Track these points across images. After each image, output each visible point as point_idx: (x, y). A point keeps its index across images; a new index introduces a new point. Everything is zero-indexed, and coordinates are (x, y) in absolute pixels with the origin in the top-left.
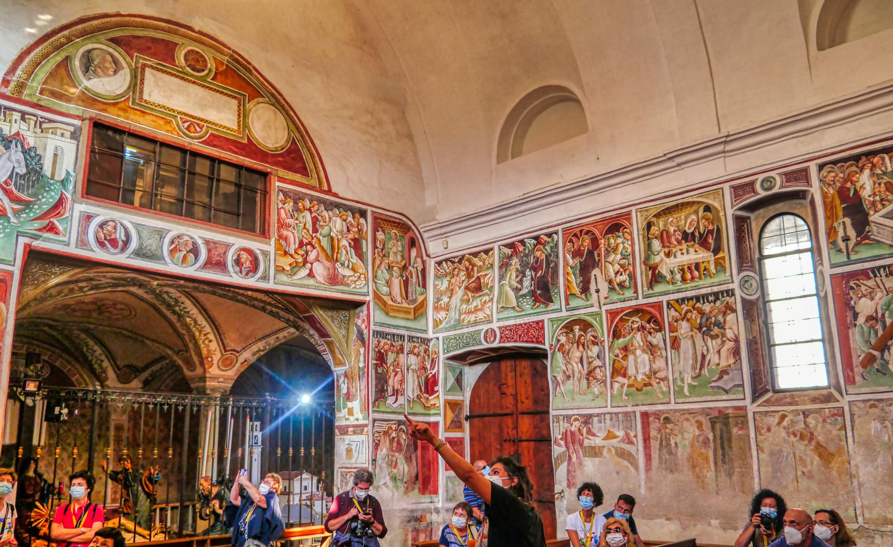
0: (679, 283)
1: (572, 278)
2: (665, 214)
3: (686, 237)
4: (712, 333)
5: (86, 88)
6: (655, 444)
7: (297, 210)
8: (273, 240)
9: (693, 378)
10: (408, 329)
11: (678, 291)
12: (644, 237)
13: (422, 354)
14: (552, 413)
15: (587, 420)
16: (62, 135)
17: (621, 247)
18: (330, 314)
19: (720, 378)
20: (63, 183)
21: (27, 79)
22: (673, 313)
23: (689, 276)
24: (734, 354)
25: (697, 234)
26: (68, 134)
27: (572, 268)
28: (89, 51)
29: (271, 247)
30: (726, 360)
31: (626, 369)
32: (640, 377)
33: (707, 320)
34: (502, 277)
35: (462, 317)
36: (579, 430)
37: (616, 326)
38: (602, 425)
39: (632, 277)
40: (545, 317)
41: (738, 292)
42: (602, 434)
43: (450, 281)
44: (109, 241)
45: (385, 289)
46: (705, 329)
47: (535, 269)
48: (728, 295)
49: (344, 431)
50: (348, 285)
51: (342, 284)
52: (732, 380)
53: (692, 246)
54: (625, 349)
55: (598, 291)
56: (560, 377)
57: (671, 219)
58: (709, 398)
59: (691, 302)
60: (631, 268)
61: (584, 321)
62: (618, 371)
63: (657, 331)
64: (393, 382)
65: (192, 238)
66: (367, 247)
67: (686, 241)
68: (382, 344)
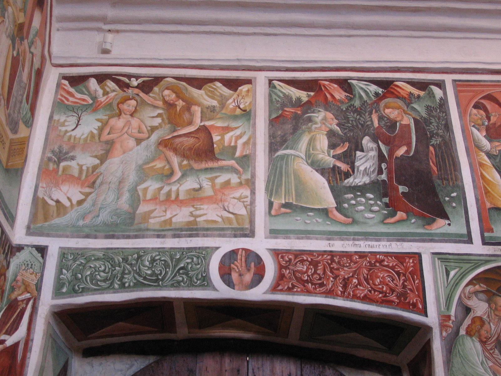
27: (489, 155)
35: (143, 208)
40: (426, 249)
43: (105, 124)
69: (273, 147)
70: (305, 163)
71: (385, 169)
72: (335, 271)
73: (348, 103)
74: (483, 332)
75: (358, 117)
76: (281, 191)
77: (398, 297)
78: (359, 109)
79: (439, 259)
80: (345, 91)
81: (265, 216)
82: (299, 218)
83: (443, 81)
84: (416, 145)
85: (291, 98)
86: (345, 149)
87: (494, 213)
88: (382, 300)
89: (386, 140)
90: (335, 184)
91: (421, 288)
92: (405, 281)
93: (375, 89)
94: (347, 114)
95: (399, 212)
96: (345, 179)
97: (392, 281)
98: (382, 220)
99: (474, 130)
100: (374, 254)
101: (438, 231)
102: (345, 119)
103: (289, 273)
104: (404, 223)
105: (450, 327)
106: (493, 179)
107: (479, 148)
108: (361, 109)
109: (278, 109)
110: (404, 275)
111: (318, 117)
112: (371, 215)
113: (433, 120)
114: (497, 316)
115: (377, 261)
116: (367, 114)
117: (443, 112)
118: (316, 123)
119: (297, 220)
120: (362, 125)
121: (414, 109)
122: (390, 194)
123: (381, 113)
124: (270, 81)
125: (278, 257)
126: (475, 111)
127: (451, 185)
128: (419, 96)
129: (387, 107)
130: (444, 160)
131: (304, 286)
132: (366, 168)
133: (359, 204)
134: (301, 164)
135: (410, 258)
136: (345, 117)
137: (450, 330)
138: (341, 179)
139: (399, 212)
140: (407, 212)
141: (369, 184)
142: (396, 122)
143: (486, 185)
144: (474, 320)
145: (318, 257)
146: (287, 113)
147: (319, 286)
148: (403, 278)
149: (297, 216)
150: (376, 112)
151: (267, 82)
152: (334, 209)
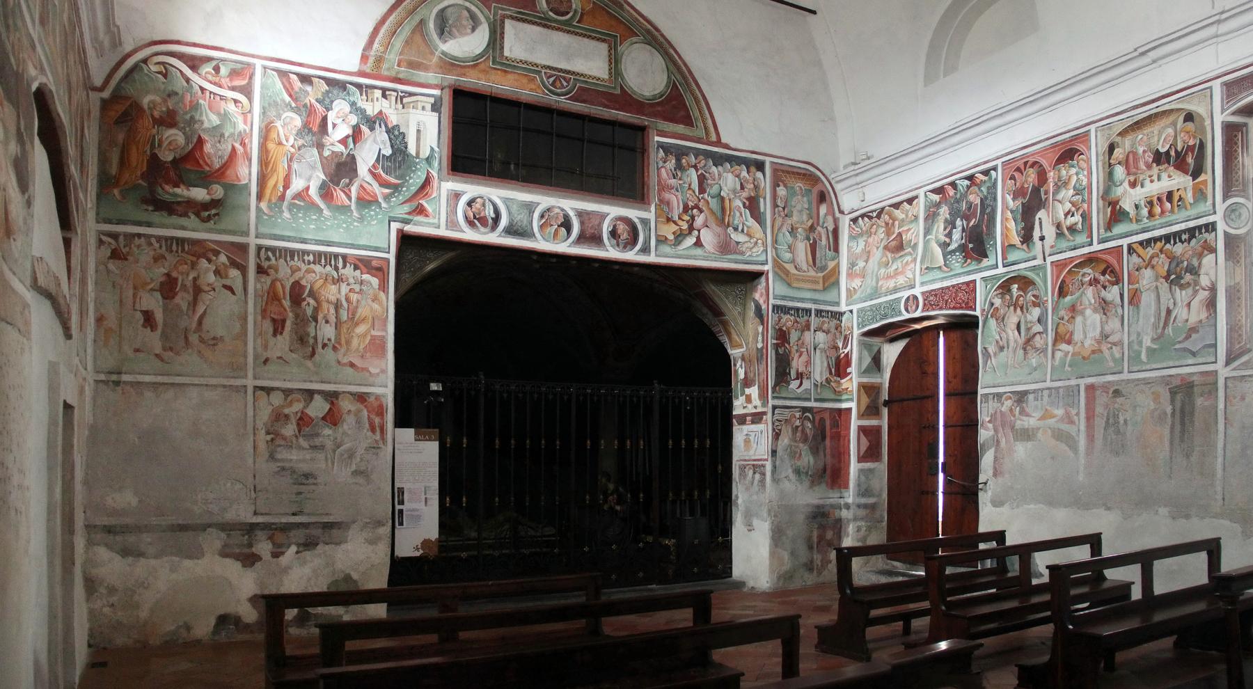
0: (1145, 220)
2: (1133, 130)
3: (1159, 158)
5: (443, 53)
6: (1099, 423)
7: (679, 167)
8: (653, 208)
9: (1153, 340)
10: (815, 301)
11: (1144, 231)
13: (833, 330)
14: (981, 391)
15: (1021, 397)
16: (423, 108)
17: (1074, 178)
18: (723, 288)
19: (1188, 337)
20: (429, 160)
21: (384, 52)
22: (1135, 258)
23: (1157, 210)
24: (1207, 306)
25: (1173, 153)
26: (429, 107)
27: (1012, 212)
28: (443, 10)
29: (651, 215)
30: (1197, 314)
31: (1072, 333)
32: (1088, 343)
33: (1177, 265)
34: (927, 231)
36: (1011, 410)
37: (1063, 282)
38: (1039, 403)
39: (1086, 217)
40: (977, 277)
41: (1221, 227)
42: (1037, 415)
44: (479, 220)
45: (788, 256)
47: (967, 218)
48: (1207, 231)
49: (742, 420)
50: (743, 253)
51: (735, 253)
54: (1073, 308)
55: (1042, 238)
56: (991, 349)
58: (1171, 364)
59: (1159, 245)
60: (1085, 206)
61: (1025, 277)
62: (1062, 337)
63: (1113, 284)
64: (797, 364)
65: (563, 210)
66: (766, 206)
68: (783, 321)
69: (925, 235)
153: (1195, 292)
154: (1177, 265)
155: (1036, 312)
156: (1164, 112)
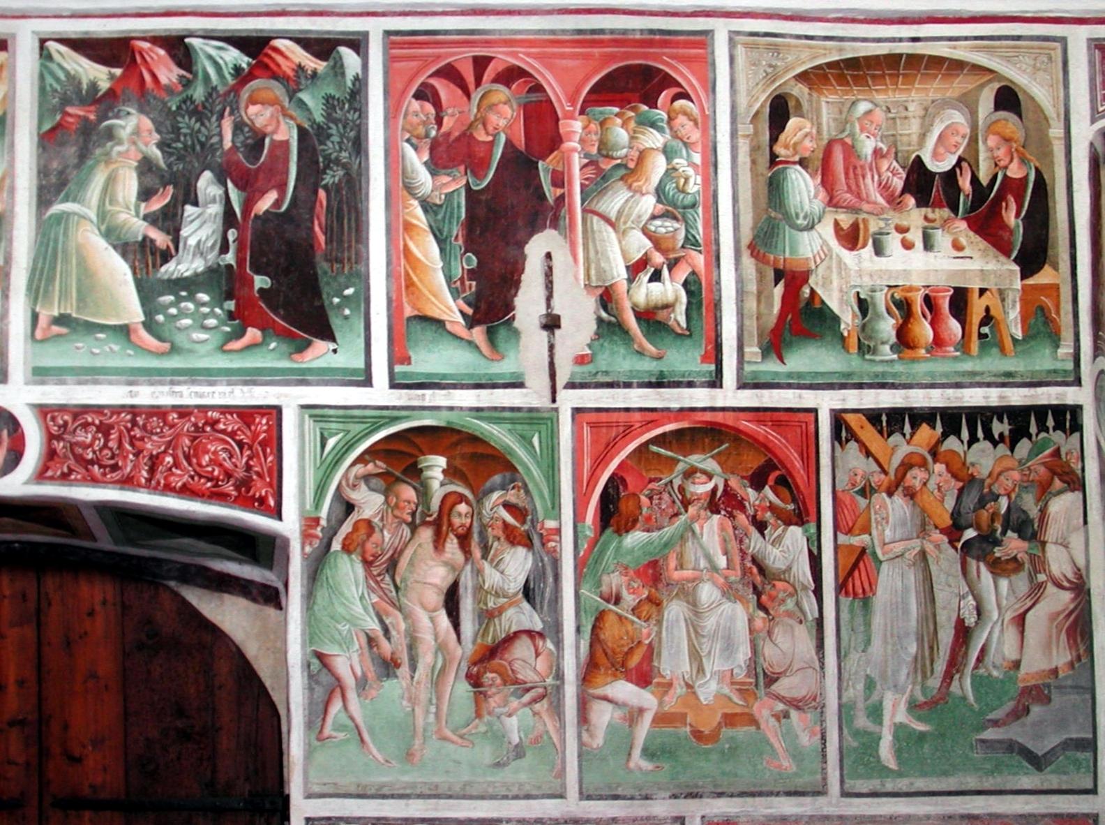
0: (886, 352)
1: (428, 250)
2: (842, 80)
3: (921, 184)
4: (998, 552)
9: (913, 707)
12: (755, 149)
17: (658, 166)
23: (924, 330)
24: (1071, 633)
25: (965, 183)
27: (427, 206)
30: (1041, 653)
31: (651, 653)
32: (708, 690)
33: (982, 503)
34: (52, 187)
39: (700, 295)
46: (970, 534)
48: (1059, 426)
52: (1062, 723)
53: (945, 223)
55: (552, 324)
56: (348, 663)
57: (863, 107)
58: (972, 782)
59: (924, 429)
60: (699, 260)
61: (474, 439)
67: (922, 202)
70: (97, 232)
71: (234, 241)
72: (138, 443)
73: (181, 93)
74: (370, 546)
75: (198, 125)
76: (54, 290)
77: (237, 488)
78: (200, 108)
79: (311, 416)
80: (180, 65)
81: (25, 341)
82: (80, 345)
83: (366, 35)
84: (295, 187)
85: (80, 83)
86: (167, 201)
87: (417, 327)
88: (212, 492)
89: (242, 179)
90: (145, 276)
91: (275, 468)
92: (250, 458)
93: (236, 59)
94: (179, 119)
95: (250, 329)
96: (161, 265)
97: (230, 458)
98: (220, 343)
99: (408, 149)
100: (204, 409)
101: (315, 364)
102: (173, 132)
103: (64, 447)
104: (257, 350)
105: (317, 537)
106: (426, 256)
107: (410, 189)
108: (204, 107)
109: (53, 111)
110: (250, 448)
111: (124, 128)
112: (203, 336)
113: (334, 131)
114: (396, 517)
115: (206, 424)
116: (214, 119)
117: (355, 110)
118: (120, 143)
119: (78, 348)
120: (203, 145)
121: (301, 104)
122: (237, 293)
123: (241, 116)
124: (43, 42)
125: (45, 418)
126: (416, 105)
127: (346, 272)
128: (315, 74)
129: (253, 101)
130: (340, 218)
131: (87, 470)
132: (199, 242)
133: (183, 314)
134: (89, 234)
135: (263, 415)
136: (172, 126)
137: (316, 543)
138: (154, 266)
139: (250, 329)
140: (263, 329)
141: (203, 273)
142: (264, 136)
143: (411, 272)
144: (356, 526)
145: (111, 417)
146: (70, 120)
147: (111, 471)
148: (248, 452)
149: (78, 341)
150: (231, 113)
151: (37, 44)
152: (140, 327)
153: (1037, 590)
154: (982, 503)
155: (517, 565)
156: (936, 62)
